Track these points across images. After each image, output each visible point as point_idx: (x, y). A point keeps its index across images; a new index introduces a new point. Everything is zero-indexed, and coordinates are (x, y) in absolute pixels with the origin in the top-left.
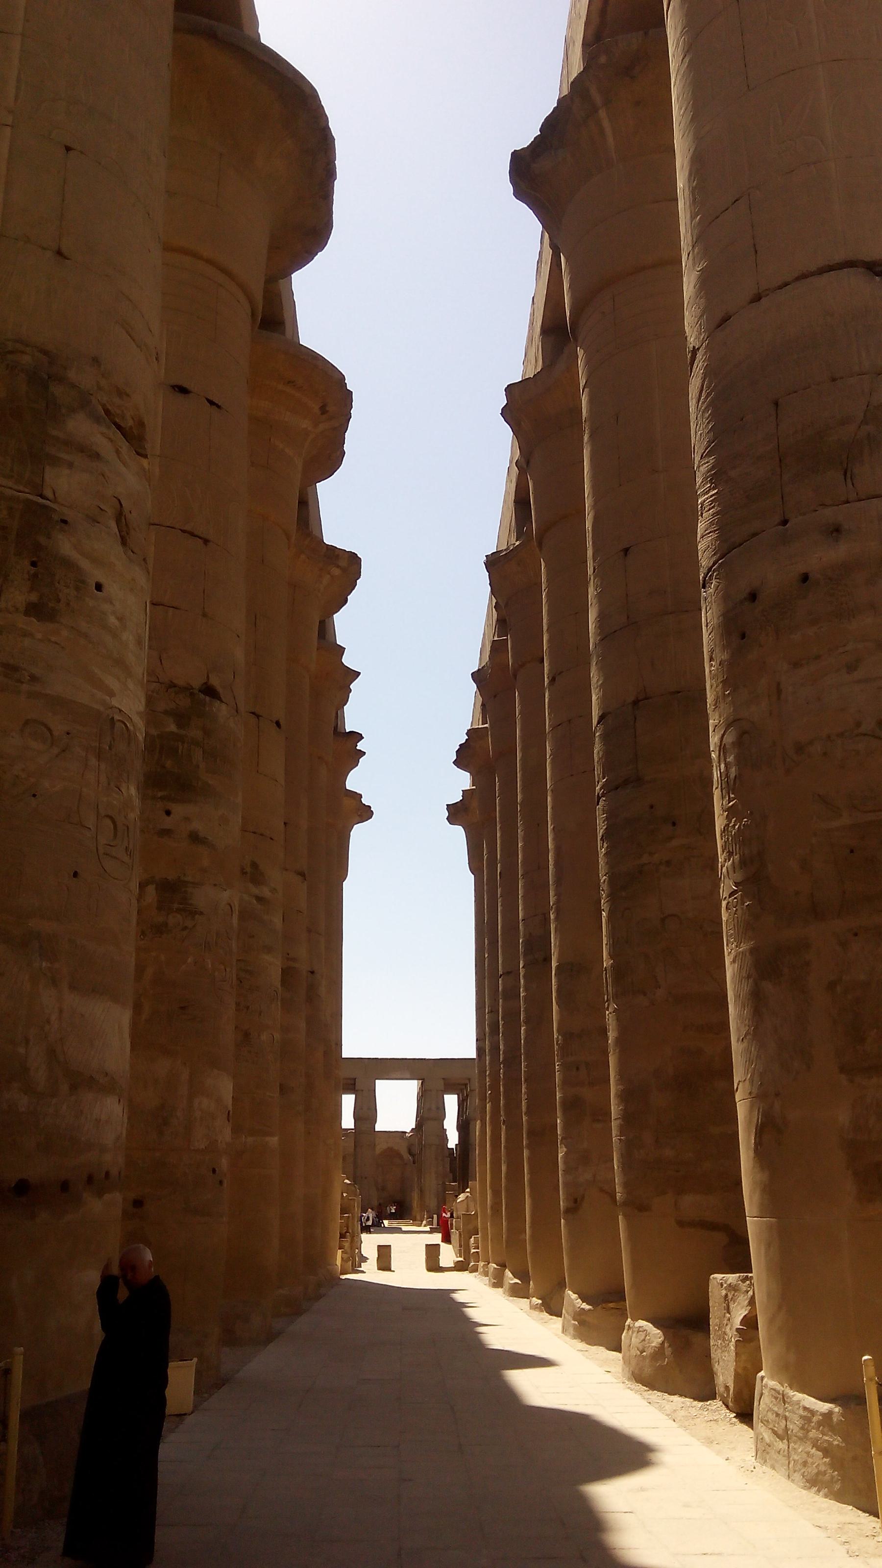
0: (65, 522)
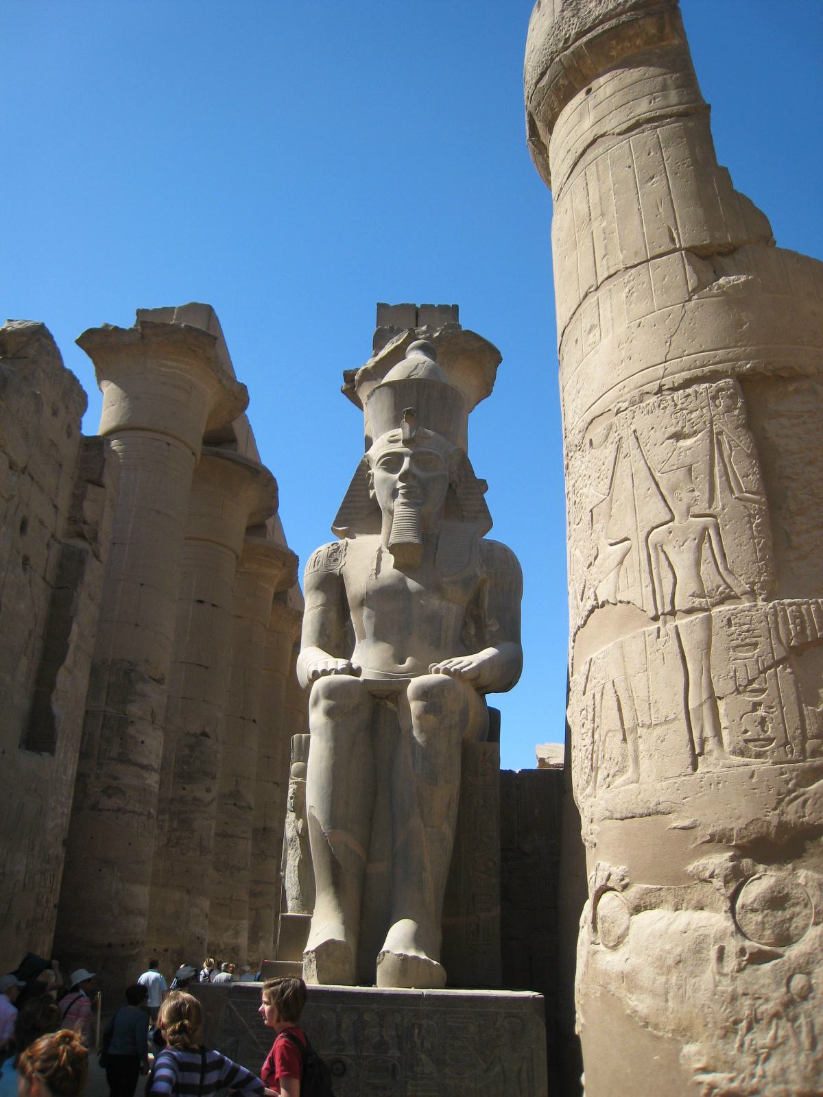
0: (132, 722)
